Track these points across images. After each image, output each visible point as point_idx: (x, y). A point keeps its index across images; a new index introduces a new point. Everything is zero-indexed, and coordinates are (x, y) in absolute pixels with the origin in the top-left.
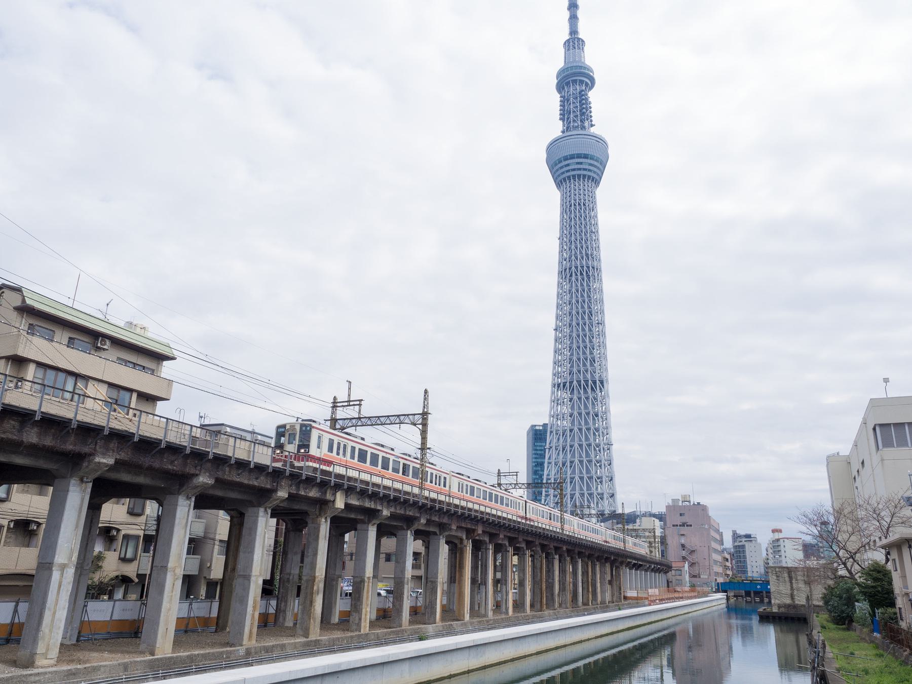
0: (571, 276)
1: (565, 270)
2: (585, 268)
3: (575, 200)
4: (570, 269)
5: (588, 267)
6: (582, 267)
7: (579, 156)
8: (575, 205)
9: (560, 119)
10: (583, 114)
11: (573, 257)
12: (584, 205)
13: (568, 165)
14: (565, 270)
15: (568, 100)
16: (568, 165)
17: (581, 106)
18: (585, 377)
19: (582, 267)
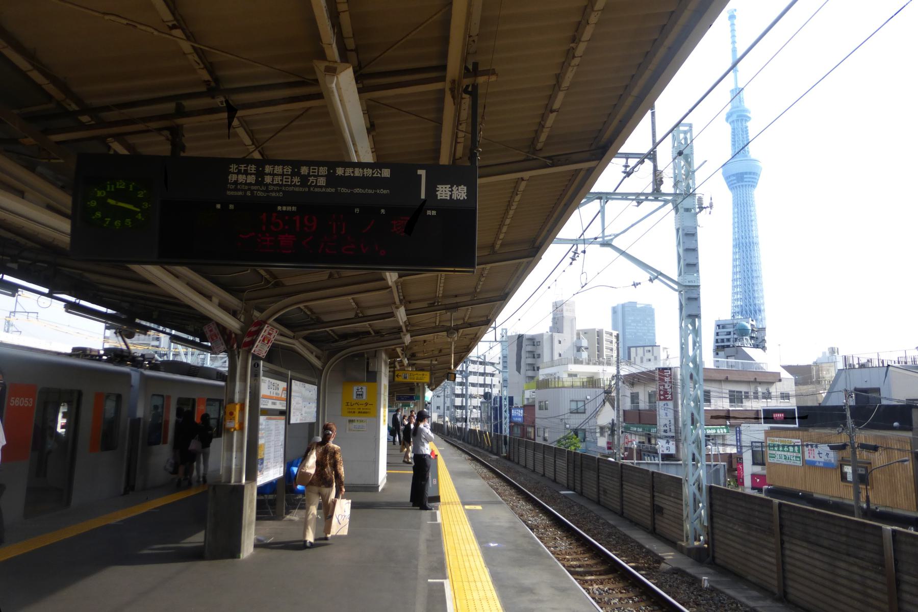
1: (736, 245)
2: (748, 244)
3: (741, 201)
4: (739, 245)
5: (750, 243)
6: (746, 243)
8: (740, 204)
14: (736, 245)
19: (746, 243)
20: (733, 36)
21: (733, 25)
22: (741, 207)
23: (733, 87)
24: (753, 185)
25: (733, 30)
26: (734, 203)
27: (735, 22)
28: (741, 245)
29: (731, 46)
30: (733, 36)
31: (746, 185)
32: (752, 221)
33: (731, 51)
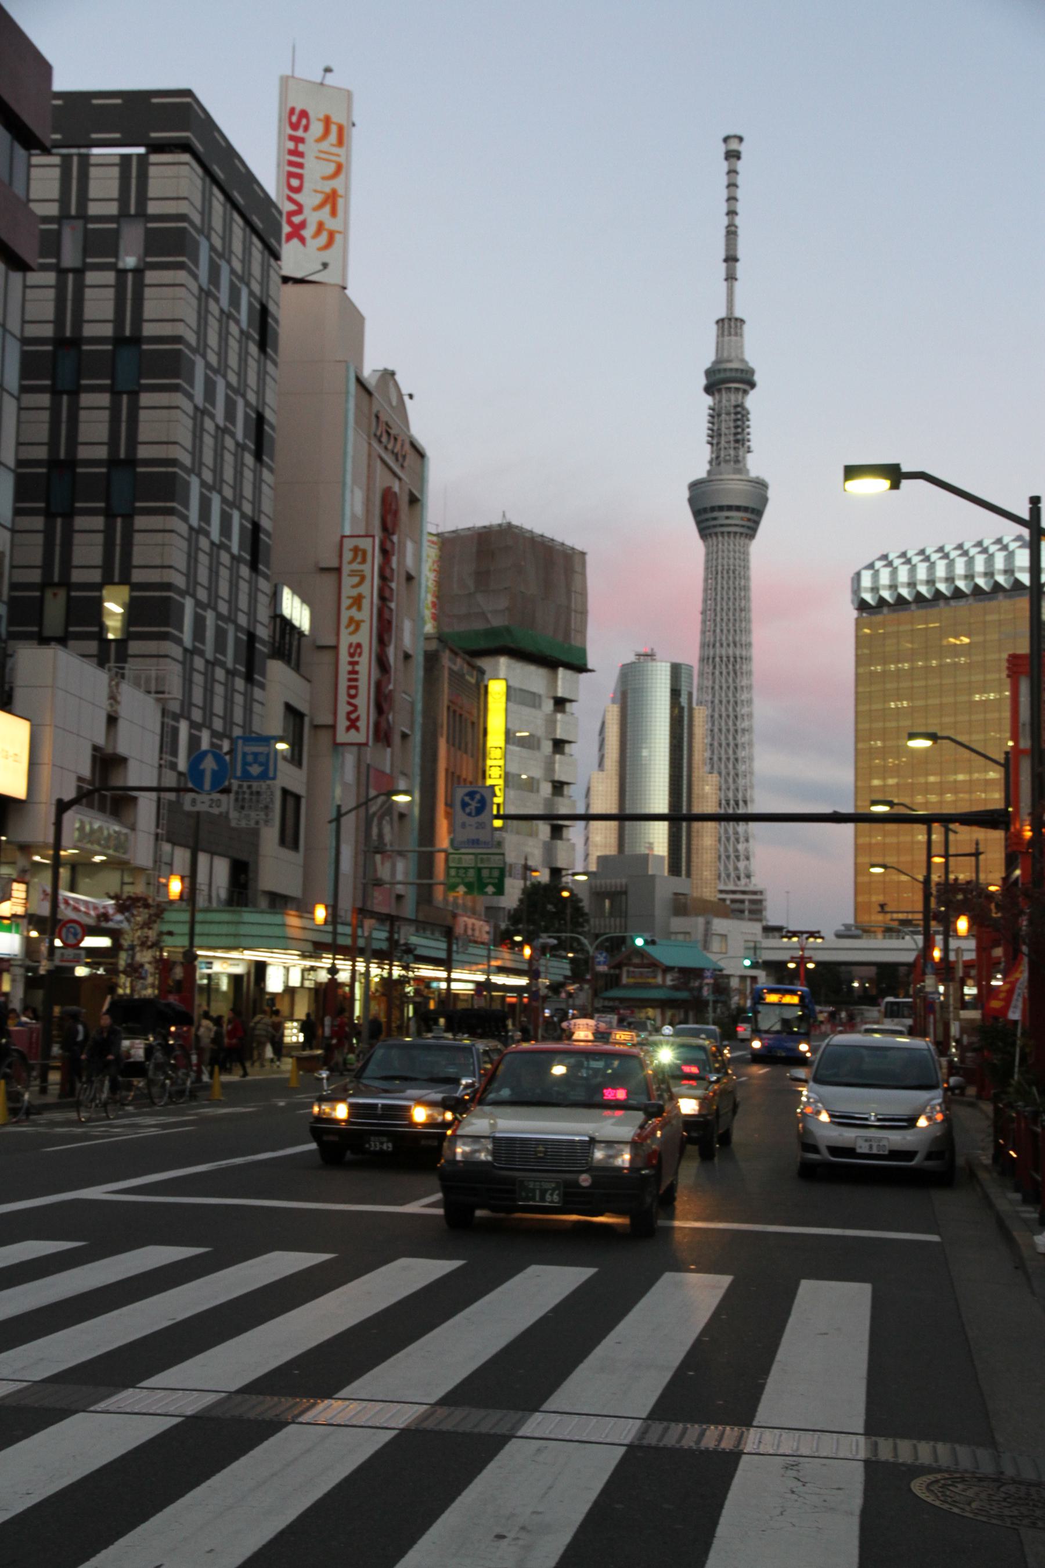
0: (714, 667)
3: (723, 566)
4: (714, 658)
5: (735, 658)
6: (728, 657)
7: (730, 508)
9: (710, 443)
10: (737, 441)
11: (718, 644)
12: (734, 572)
13: (715, 519)
15: (719, 415)
16: (715, 519)
17: (736, 427)
18: (726, 796)
19: (728, 657)
20: (732, 199)
21: (732, 172)
22: (723, 578)
23: (722, 314)
24: (751, 530)
25: (732, 185)
26: (707, 568)
27: (740, 165)
28: (717, 659)
29: (725, 221)
30: (732, 199)
31: (735, 533)
32: (741, 610)
33: (723, 232)
